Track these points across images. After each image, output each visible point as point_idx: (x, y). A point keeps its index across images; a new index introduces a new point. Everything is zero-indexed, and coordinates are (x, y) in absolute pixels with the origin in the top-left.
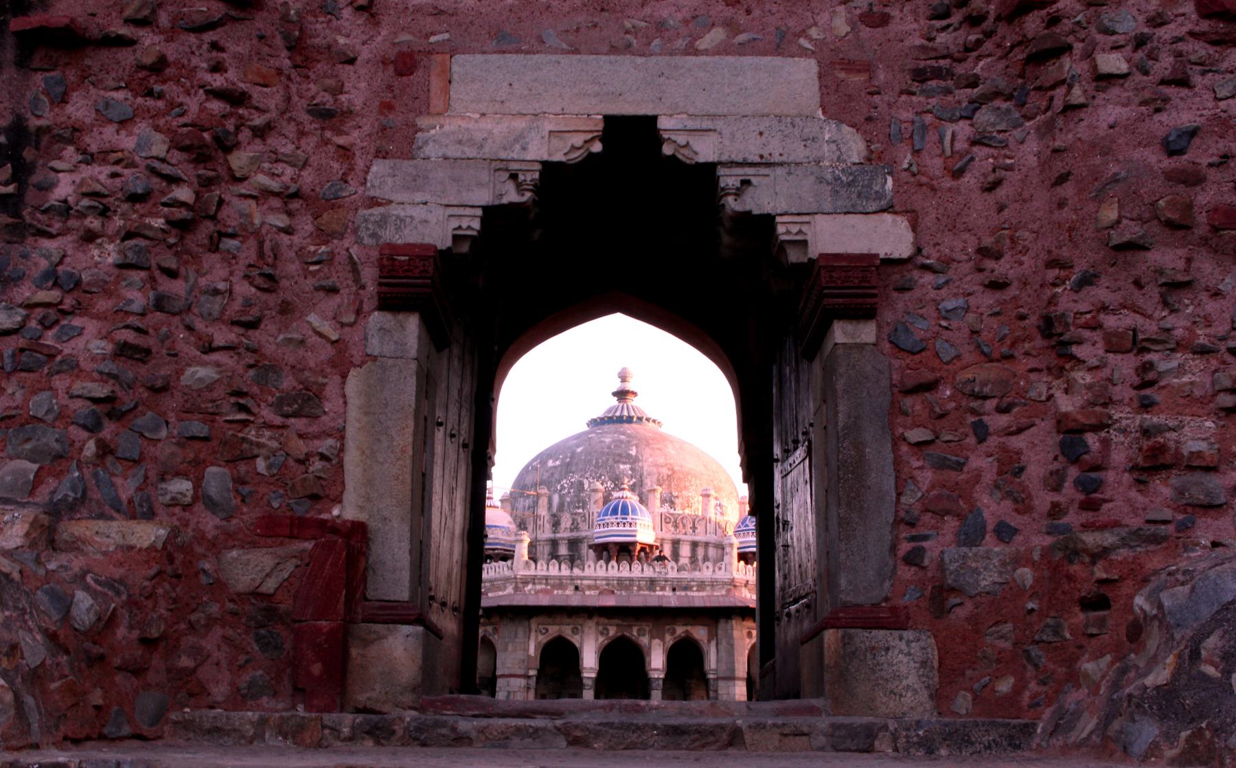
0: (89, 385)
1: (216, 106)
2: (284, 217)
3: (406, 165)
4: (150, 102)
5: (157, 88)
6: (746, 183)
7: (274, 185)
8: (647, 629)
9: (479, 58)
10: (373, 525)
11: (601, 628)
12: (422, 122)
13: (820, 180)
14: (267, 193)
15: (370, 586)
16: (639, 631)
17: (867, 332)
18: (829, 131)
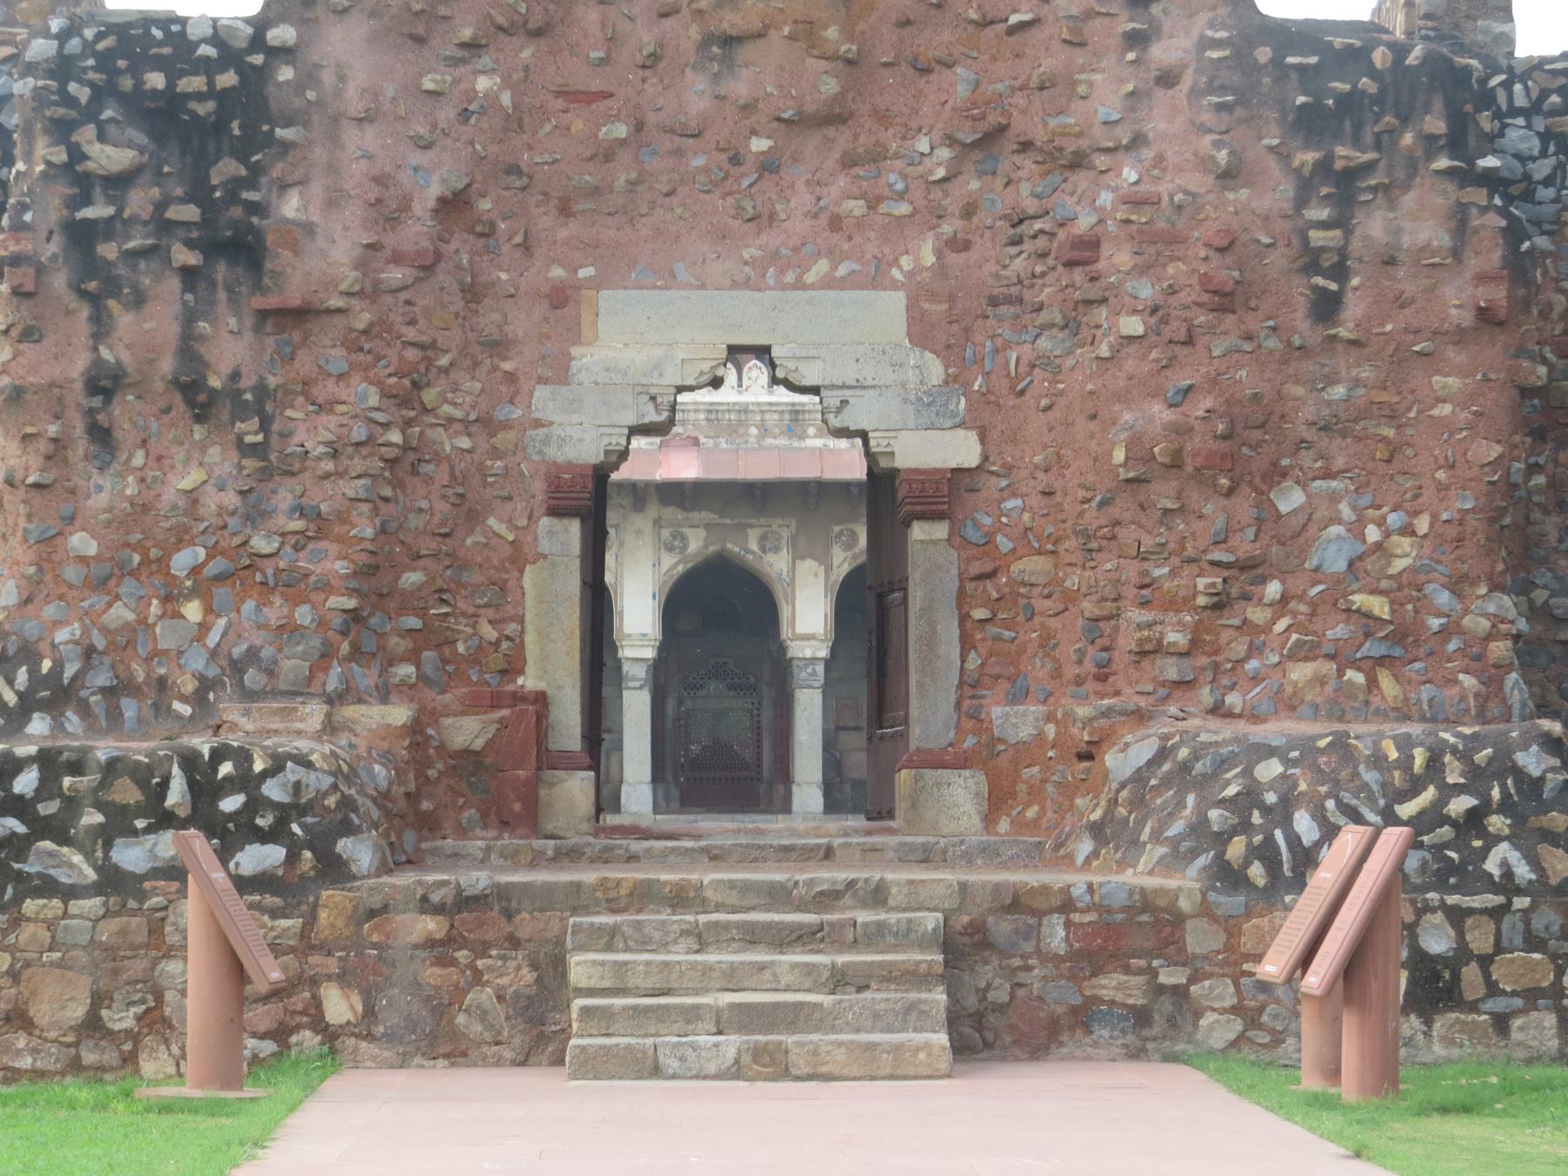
0: (341, 599)
1: (412, 354)
2: (466, 439)
3: (564, 390)
4: (361, 357)
5: (367, 346)
6: (844, 402)
7: (459, 414)
8: (785, 534)
9: (621, 293)
10: (549, 692)
11: (666, 533)
12: (575, 351)
13: (906, 401)
14: (451, 420)
15: (550, 739)
16: (763, 539)
17: (940, 530)
18: (914, 357)
